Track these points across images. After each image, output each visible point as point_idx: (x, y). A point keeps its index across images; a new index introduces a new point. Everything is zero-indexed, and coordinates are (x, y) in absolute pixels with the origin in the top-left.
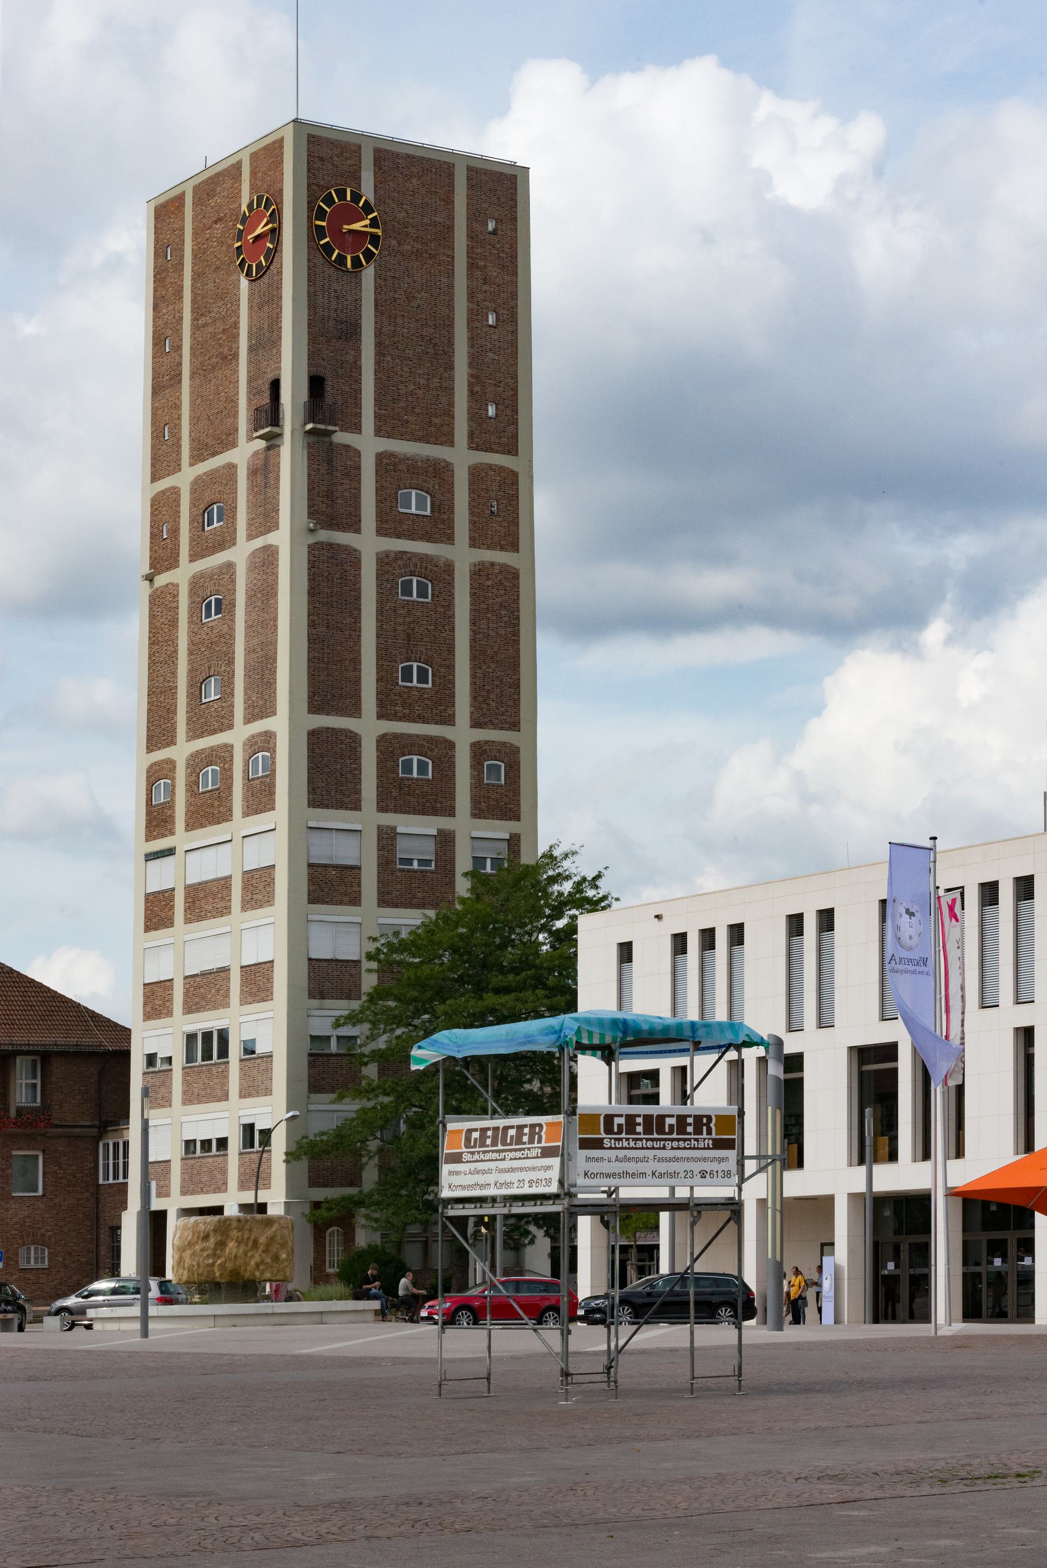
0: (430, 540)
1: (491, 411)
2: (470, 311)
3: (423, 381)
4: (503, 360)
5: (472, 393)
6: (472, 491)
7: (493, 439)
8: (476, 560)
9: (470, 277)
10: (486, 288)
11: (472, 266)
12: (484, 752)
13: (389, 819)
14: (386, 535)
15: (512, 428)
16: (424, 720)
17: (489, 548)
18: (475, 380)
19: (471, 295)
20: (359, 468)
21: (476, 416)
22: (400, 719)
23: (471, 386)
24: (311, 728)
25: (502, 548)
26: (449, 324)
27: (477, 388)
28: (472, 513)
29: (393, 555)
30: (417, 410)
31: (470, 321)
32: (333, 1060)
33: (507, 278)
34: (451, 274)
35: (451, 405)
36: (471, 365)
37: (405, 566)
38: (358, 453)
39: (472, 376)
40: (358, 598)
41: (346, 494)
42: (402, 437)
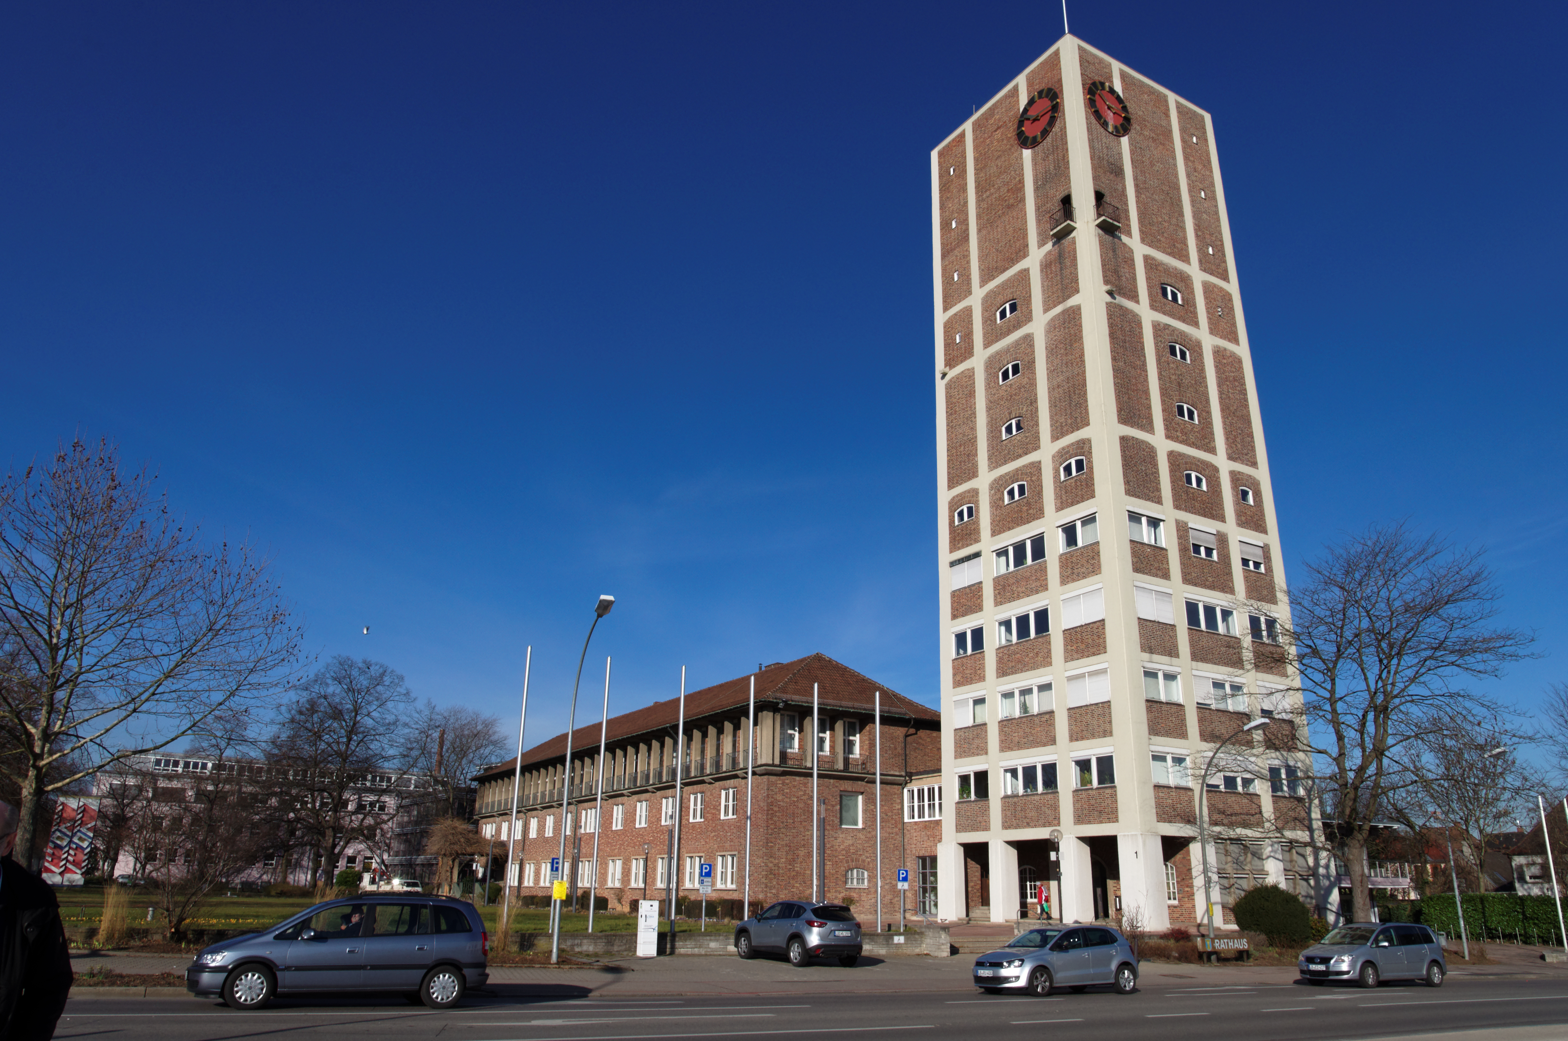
0: (1184, 321)
1: (1211, 251)
2: (1189, 185)
3: (1167, 218)
4: (1212, 221)
5: (1197, 236)
6: (1206, 298)
7: (1213, 268)
8: (1215, 344)
9: (1186, 165)
10: (1196, 174)
11: (1186, 158)
12: (1238, 480)
13: (1184, 516)
14: (1156, 310)
15: (1223, 264)
16: (1198, 448)
17: (1221, 338)
18: (1198, 228)
19: (1188, 176)
20: (1133, 260)
21: (1202, 251)
22: (1181, 442)
23: (1196, 231)
24: (1122, 434)
25: (1229, 340)
26: (1178, 189)
27: (1199, 233)
28: (1208, 312)
29: (1162, 325)
30: (1165, 235)
31: (1190, 191)
32: (1164, 707)
33: (1208, 173)
34: (1174, 158)
35: (1185, 238)
36: (1194, 217)
37: (1171, 335)
38: (1131, 251)
39: (1195, 224)
40: (1143, 349)
41: (1127, 275)
42: (1157, 248)
